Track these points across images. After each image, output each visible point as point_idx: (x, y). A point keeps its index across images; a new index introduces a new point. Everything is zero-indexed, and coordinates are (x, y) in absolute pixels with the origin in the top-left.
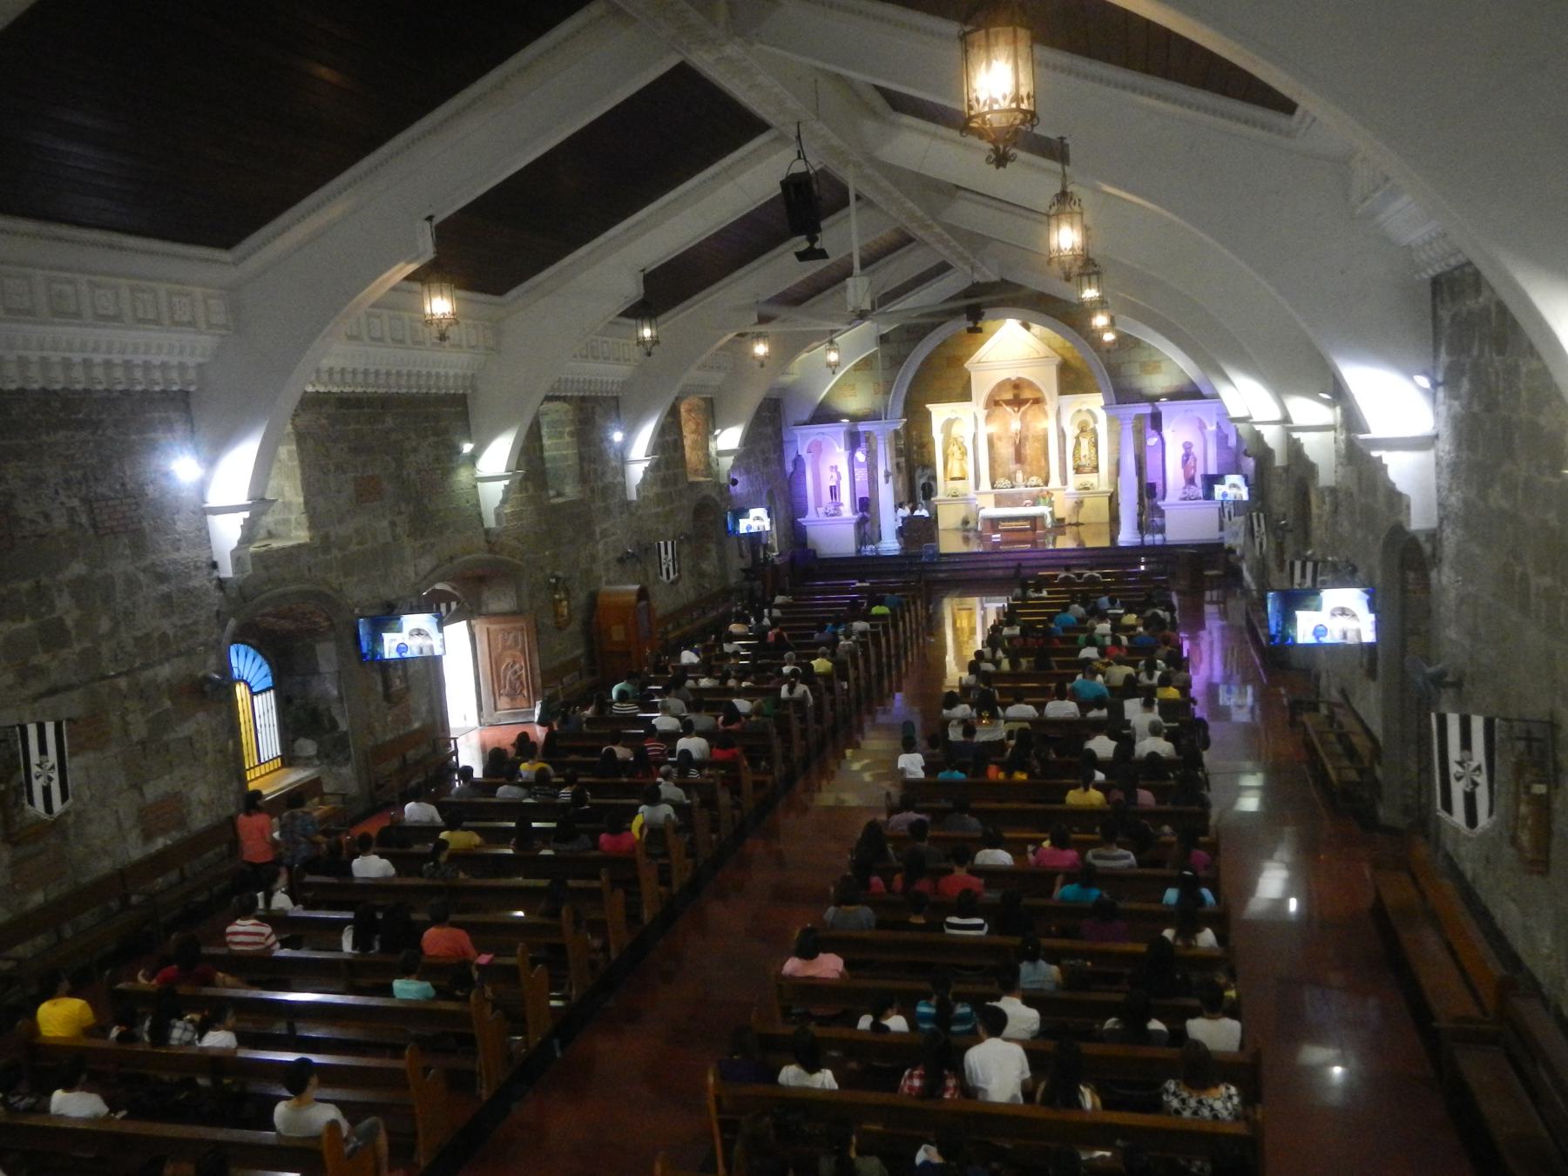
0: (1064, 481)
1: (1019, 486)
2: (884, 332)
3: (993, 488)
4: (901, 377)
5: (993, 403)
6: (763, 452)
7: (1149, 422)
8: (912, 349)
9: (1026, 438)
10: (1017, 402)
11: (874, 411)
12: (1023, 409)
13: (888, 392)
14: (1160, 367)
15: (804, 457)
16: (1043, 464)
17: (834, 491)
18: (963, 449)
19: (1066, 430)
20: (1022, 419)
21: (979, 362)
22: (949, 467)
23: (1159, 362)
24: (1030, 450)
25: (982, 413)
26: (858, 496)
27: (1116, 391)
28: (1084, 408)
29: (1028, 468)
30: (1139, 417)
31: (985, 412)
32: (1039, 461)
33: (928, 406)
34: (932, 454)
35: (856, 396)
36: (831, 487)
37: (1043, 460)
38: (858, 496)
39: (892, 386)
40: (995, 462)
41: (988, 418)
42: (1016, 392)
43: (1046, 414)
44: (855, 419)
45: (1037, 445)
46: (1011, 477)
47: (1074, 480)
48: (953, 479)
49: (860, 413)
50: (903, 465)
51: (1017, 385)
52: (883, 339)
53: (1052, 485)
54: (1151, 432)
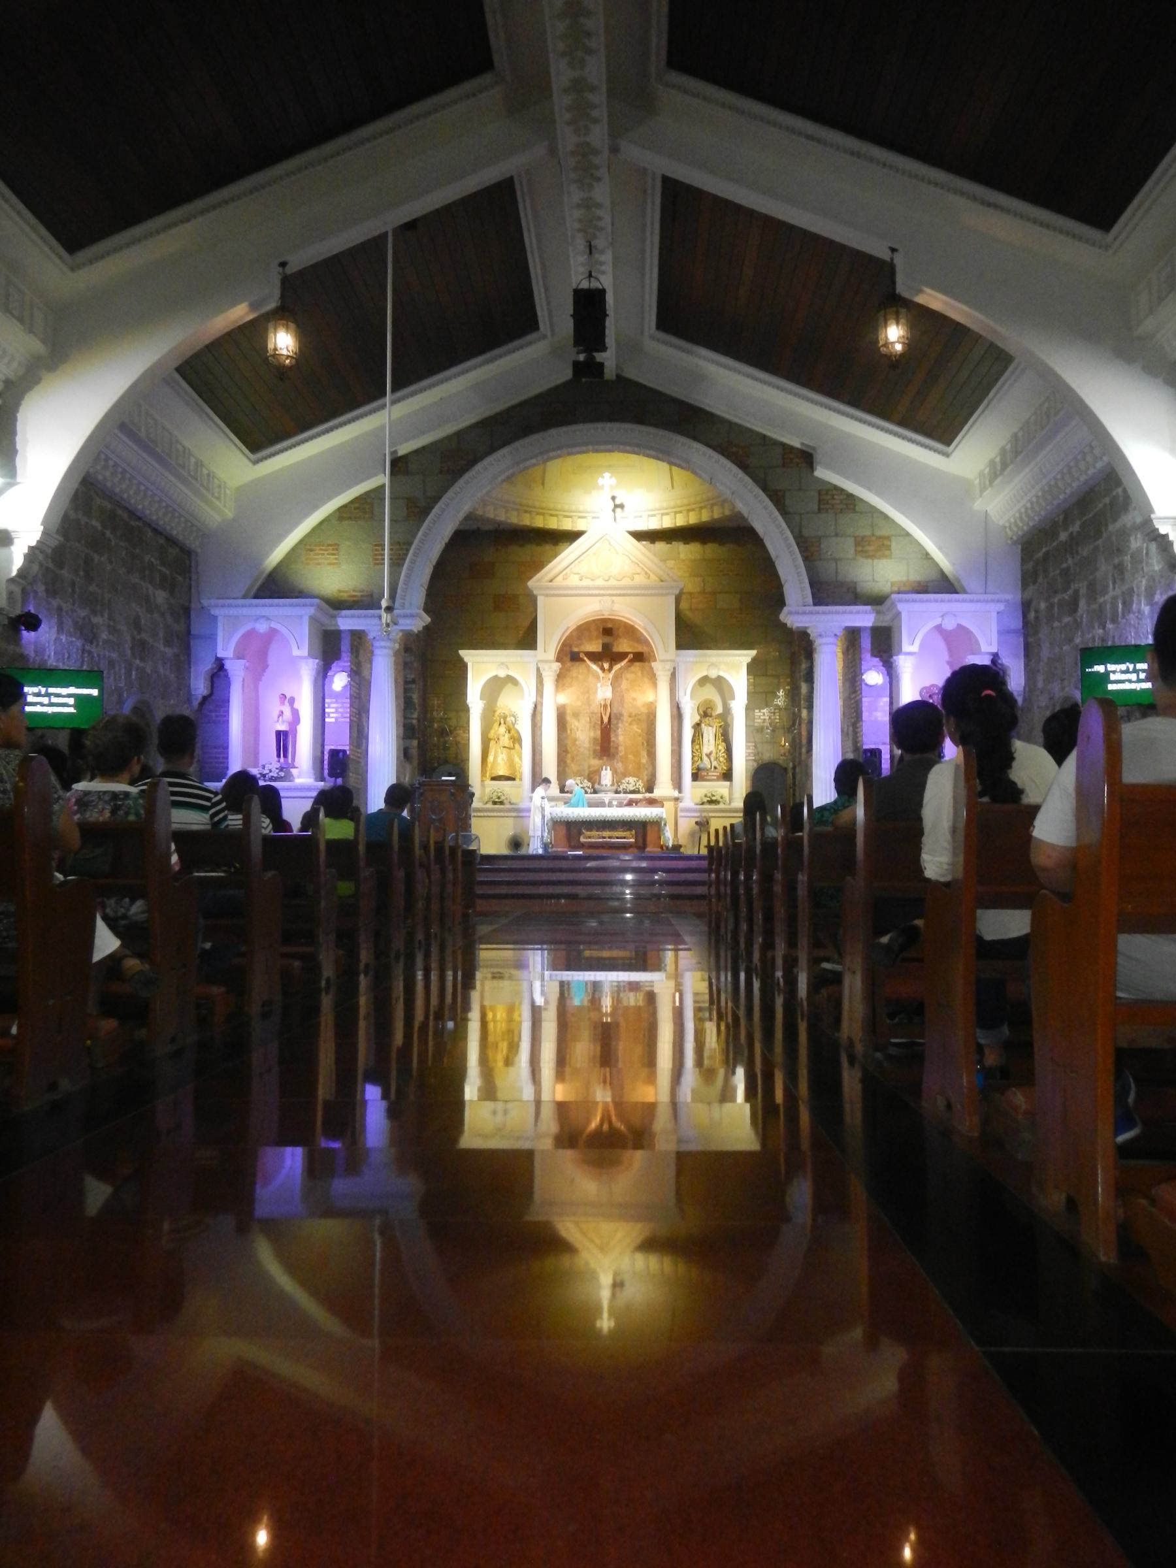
1: (606, 791)
2: (403, 450)
4: (425, 535)
5: (570, 655)
6: (136, 624)
7: (866, 642)
8: (445, 489)
9: (619, 717)
10: (608, 656)
12: (617, 667)
13: (397, 562)
14: (889, 548)
15: (228, 665)
16: (644, 761)
17: (284, 741)
18: (513, 732)
19: (682, 705)
20: (616, 680)
21: (551, 581)
22: (491, 758)
23: (888, 538)
24: (623, 737)
25: (551, 670)
26: (327, 748)
27: (812, 585)
28: (713, 674)
29: (620, 766)
30: (852, 636)
31: (557, 666)
32: (637, 755)
33: (462, 653)
34: (462, 748)
35: (339, 564)
36: (279, 734)
37: (644, 753)
38: (327, 748)
39: (408, 550)
40: (566, 751)
41: (560, 678)
42: (607, 639)
43: (653, 678)
44: (337, 605)
45: (635, 727)
46: (593, 777)
47: (692, 793)
48: (494, 779)
49: (345, 596)
50: (414, 752)
51: (608, 629)
52: (399, 465)
53: (657, 793)
54: (868, 660)
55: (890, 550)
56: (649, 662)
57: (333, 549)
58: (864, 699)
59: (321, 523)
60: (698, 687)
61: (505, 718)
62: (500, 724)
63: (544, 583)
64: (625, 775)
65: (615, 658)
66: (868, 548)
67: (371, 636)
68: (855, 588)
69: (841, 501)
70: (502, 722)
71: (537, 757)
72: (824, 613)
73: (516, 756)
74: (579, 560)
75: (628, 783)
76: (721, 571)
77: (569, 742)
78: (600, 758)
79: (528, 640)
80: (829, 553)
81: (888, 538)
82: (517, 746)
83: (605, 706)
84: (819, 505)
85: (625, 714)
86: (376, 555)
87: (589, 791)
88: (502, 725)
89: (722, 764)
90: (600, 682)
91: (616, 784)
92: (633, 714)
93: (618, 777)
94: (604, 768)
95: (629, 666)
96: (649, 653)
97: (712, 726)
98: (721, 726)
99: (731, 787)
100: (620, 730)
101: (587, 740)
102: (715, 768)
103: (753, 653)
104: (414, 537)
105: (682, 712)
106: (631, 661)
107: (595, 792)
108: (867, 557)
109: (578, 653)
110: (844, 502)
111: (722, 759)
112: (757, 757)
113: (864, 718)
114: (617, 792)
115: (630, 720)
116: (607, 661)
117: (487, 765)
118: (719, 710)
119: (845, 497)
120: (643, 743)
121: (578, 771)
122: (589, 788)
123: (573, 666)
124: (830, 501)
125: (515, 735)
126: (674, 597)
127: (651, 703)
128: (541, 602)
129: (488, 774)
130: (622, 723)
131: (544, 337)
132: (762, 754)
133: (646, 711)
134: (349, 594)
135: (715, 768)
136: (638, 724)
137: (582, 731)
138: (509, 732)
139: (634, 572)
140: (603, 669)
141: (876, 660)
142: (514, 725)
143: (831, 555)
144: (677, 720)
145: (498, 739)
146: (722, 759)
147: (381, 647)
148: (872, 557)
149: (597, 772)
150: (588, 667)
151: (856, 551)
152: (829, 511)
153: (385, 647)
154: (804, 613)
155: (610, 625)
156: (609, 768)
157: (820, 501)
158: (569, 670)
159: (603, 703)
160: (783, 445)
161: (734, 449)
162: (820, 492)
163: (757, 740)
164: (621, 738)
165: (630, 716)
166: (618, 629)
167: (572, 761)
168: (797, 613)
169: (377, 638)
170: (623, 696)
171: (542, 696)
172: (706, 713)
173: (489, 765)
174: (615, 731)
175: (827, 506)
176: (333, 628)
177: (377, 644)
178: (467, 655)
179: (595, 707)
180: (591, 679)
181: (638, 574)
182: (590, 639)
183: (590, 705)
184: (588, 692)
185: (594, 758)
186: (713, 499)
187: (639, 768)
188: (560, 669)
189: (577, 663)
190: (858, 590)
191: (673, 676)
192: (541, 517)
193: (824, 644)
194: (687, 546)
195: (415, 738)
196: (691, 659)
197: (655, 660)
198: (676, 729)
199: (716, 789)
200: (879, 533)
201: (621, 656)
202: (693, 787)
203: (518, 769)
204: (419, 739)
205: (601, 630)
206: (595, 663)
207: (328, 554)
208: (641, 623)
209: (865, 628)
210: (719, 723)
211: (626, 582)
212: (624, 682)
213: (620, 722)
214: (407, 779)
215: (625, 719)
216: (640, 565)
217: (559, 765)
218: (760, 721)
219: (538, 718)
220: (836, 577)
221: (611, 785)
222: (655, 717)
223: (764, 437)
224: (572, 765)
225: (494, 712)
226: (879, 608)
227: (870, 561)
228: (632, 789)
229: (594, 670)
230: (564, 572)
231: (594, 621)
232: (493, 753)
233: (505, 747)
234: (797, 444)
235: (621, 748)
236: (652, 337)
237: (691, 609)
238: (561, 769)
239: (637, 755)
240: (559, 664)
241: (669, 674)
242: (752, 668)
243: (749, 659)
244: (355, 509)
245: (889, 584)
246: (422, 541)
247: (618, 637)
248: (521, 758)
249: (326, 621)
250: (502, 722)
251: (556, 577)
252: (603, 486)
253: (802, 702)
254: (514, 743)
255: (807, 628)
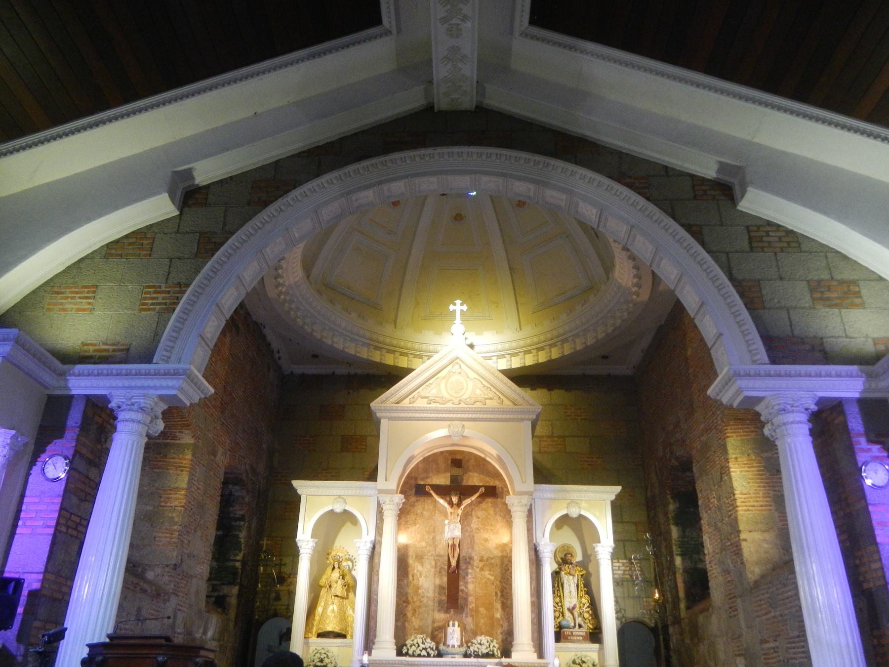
0: (540, 651)
1: (453, 654)
3: (399, 653)
4: (215, 271)
7: (855, 423)
9: (469, 560)
11: (128, 350)
12: (467, 501)
14: (858, 294)
16: (498, 615)
18: (347, 578)
19: (541, 548)
20: (465, 519)
21: (398, 403)
22: (319, 610)
25: (394, 502)
28: (574, 512)
31: (399, 498)
32: (489, 607)
33: (296, 483)
37: (498, 606)
40: (407, 602)
41: (403, 514)
42: (457, 471)
45: (487, 573)
46: (437, 634)
48: (320, 635)
50: (233, 601)
55: (861, 297)
56: (502, 498)
57: (88, 293)
58: (871, 508)
59: (81, 260)
60: (555, 529)
61: (340, 563)
62: (334, 568)
63: (388, 404)
64: (475, 634)
65: (465, 492)
66: (828, 295)
67: (113, 405)
68: (822, 344)
69: (780, 238)
70: (336, 566)
71: (373, 608)
72: (788, 375)
73: (349, 608)
74: (427, 383)
75: (480, 644)
76: (569, 416)
77: (410, 591)
78: (447, 612)
79: (372, 476)
80: (776, 301)
81: (854, 282)
82: (351, 595)
83: (453, 546)
84: (750, 243)
85: (475, 558)
86: (145, 299)
87: (432, 653)
88: (337, 570)
89: (587, 621)
90: (447, 518)
91: (465, 645)
92: (485, 558)
93: (468, 637)
94: (451, 623)
95: (480, 502)
96: (502, 488)
97: (573, 576)
98: (582, 575)
99: (601, 652)
100: (470, 576)
101: (432, 587)
102: (580, 626)
103: (618, 489)
104: (197, 272)
105: (541, 555)
106: (483, 496)
107: (440, 655)
108: (830, 306)
109: (424, 486)
110: (783, 239)
111: (586, 615)
112: (620, 615)
113: (879, 539)
114: (466, 655)
115: (481, 564)
116: (456, 495)
117: (314, 619)
118: (579, 557)
119: (783, 234)
120: (496, 593)
121: (420, 627)
122: (432, 649)
123: (417, 501)
124: (765, 239)
125: (351, 582)
126: (529, 424)
127: (506, 544)
128: (384, 424)
129: (315, 629)
130: (472, 568)
131: (388, 33)
132: (625, 612)
133: (500, 554)
134: (97, 347)
135: (580, 626)
136: (490, 570)
137: (426, 577)
138: (343, 578)
139: (486, 396)
140: (451, 504)
141: (876, 449)
142: (350, 570)
143: (779, 302)
144: (534, 566)
145: (330, 587)
146: (586, 615)
147: (127, 421)
148: (836, 306)
149: (443, 628)
150: (435, 501)
151: (814, 299)
152: (765, 249)
153: (133, 421)
154: (758, 375)
155: (458, 457)
156: (456, 623)
157: (750, 238)
158: (413, 506)
159: (450, 543)
160: (692, 176)
161: (628, 180)
162: (747, 227)
163: (618, 595)
164: (471, 587)
165: (481, 560)
166: (468, 461)
167: (413, 614)
168: (748, 375)
169: (124, 407)
170: (473, 536)
171: (381, 535)
172: (564, 560)
173: (317, 618)
174: (464, 578)
175: (760, 244)
176: (65, 392)
177: (122, 416)
178: (300, 485)
179: (442, 549)
180: (438, 516)
181: (492, 399)
182: (438, 472)
183: (435, 547)
184: (434, 532)
185: (439, 611)
186: (565, 334)
187: (492, 626)
188: (404, 503)
189: (422, 499)
190: (828, 348)
191: (530, 514)
192: (392, 356)
193: (792, 423)
194: (535, 392)
195: (235, 585)
196: (549, 495)
197: (509, 494)
198: (534, 576)
199: (584, 653)
200: (839, 277)
201: (472, 490)
202: (557, 650)
203: (350, 624)
204: (241, 585)
205: (449, 462)
206: (443, 498)
207: (80, 298)
208: (494, 452)
209: (849, 400)
210: (581, 571)
211: (478, 405)
212: (475, 520)
213: (469, 567)
214: (210, 634)
215: (475, 564)
216: (493, 389)
217: (397, 620)
218: (619, 572)
219: (376, 560)
220: (792, 331)
221: (459, 646)
222: (510, 561)
223: (666, 167)
224: (413, 619)
225: (328, 554)
226: (870, 368)
227: (836, 311)
228: (485, 651)
229: (443, 506)
230: (411, 396)
231: (442, 453)
232: (323, 604)
233: (337, 596)
234: (709, 171)
235: (471, 599)
236: (524, 34)
237: (540, 452)
238: (399, 624)
239: (489, 607)
240: (403, 496)
241: (526, 509)
242: (617, 508)
243: (613, 497)
244: (130, 244)
245: (870, 340)
246: (209, 278)
247: (467, 470)
248: (353, 610)
249: (47, 377)
250: (336, 566)
251: (402, 400)
252: (455, 311)
253: (674, 548)
254: (348, 591)
255: (759, 400)
